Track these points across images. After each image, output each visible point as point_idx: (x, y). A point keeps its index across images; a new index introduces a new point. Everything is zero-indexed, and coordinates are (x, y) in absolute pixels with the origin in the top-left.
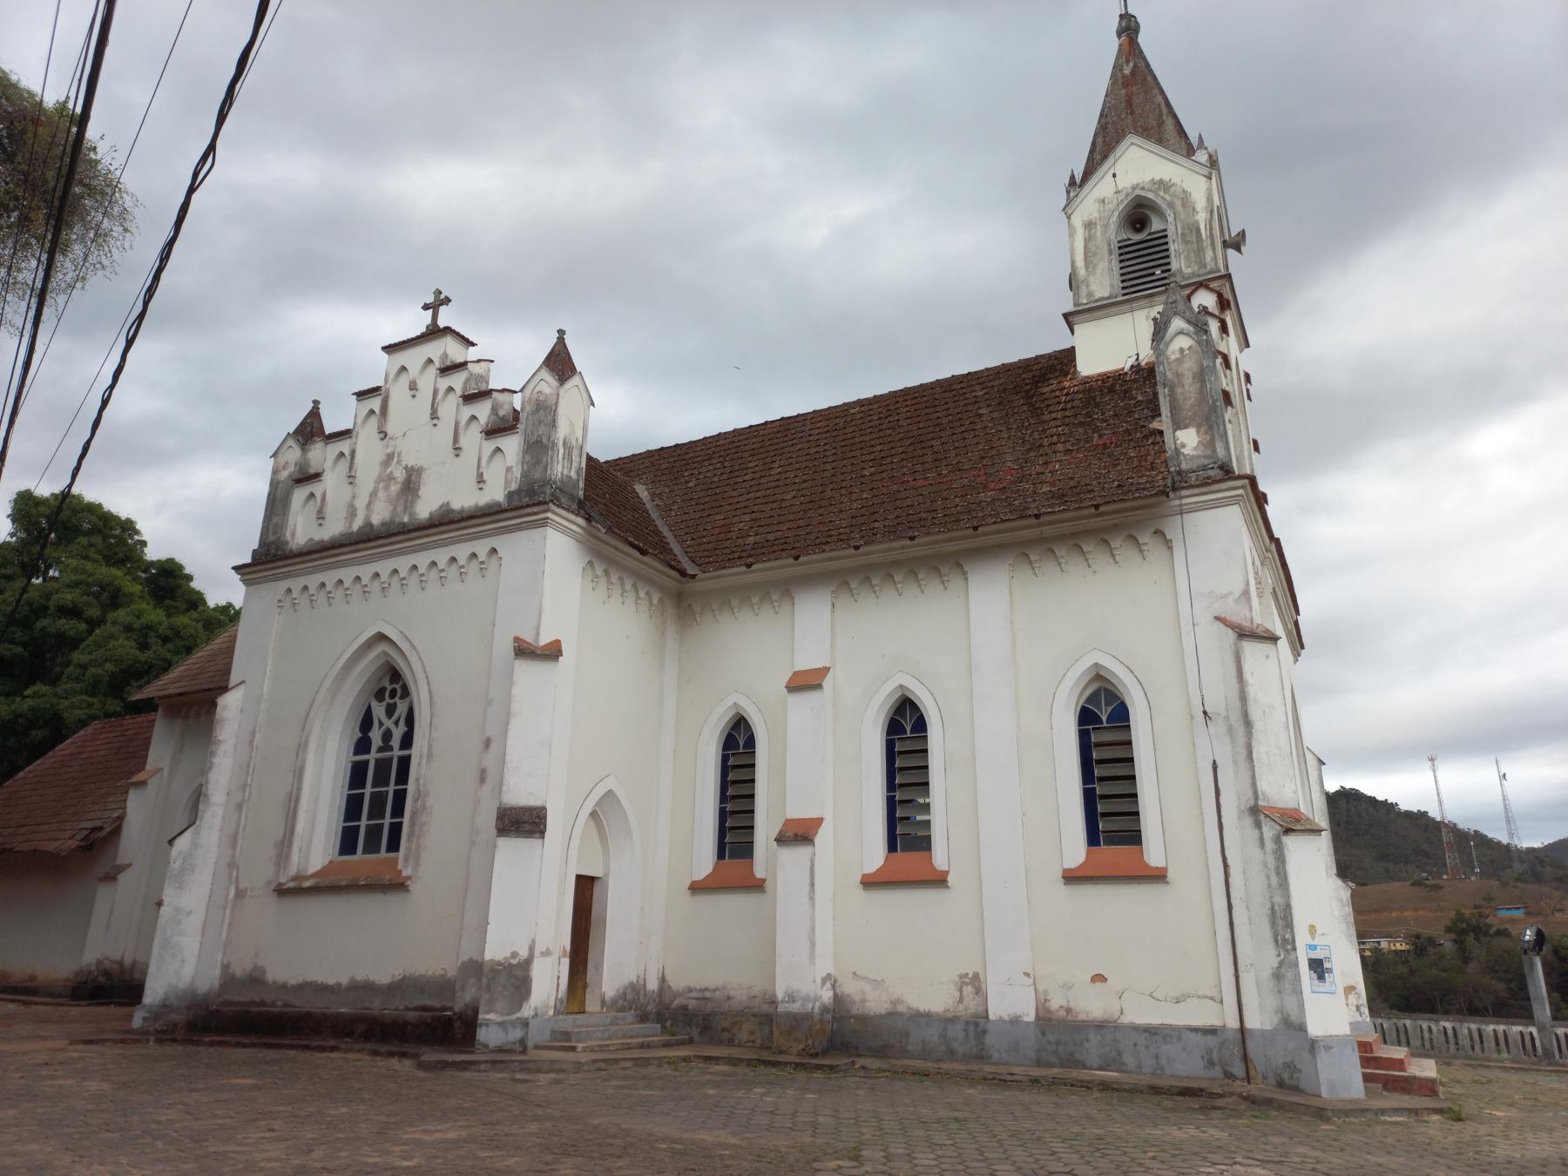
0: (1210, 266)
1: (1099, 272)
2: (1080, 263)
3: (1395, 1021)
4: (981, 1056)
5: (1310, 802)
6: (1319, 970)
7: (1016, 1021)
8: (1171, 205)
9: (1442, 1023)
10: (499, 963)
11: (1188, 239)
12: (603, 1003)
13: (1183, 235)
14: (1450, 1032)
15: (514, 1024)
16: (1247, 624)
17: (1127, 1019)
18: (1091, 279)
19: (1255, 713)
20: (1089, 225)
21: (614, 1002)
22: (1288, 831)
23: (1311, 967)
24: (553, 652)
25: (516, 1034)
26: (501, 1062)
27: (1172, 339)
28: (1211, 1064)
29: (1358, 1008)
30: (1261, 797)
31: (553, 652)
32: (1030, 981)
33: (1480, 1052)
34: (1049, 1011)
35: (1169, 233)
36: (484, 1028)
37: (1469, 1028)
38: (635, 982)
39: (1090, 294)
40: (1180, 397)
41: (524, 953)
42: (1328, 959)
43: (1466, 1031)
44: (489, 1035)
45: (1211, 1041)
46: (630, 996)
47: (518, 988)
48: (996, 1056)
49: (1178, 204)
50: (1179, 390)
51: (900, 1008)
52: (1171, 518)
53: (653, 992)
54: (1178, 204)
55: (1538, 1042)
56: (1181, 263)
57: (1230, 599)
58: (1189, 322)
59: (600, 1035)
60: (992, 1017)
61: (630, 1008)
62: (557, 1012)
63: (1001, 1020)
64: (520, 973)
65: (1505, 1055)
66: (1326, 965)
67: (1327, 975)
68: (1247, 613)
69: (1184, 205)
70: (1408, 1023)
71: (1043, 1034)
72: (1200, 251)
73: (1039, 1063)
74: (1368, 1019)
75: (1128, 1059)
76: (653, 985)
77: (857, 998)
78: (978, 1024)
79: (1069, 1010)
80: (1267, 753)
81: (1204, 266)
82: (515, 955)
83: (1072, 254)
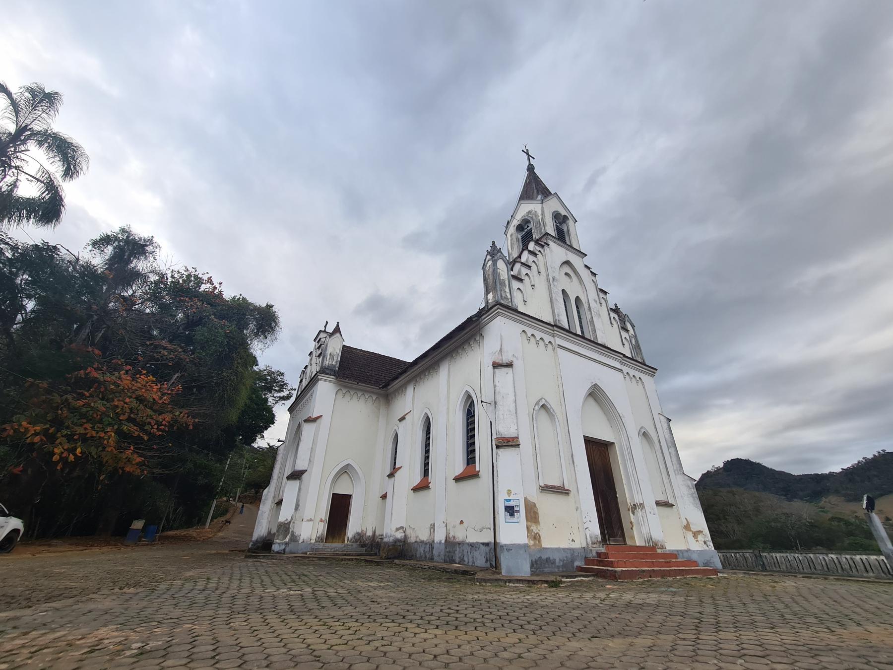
0: (544, 233)
1: (514, 248)
2: (510, 249)
3: (805, 555)
4: (432, 559)
5: (627, 438)
6: (510, 511)
7: (440, 543)
8: (532, 218)
9: (830, 555)
10: (282, 523)
11: (537, 226)
12: (348, 539)
13: (536, 226)
14: (836, 561)
15: (282, 543)
16: (501, 362)
17: (468, 541)
18: (513, 252)
19: (499, 398)
20: (511, 235)
21: (351, 539)
22: (498, 447)
23: (506, 510)
24: (315, 420)
25: (283, 547)
26: (267, 556)
27: (487, 264)
28: (487, 560)
29: (705, 542)
30: (498, 434)
31: (315, 420)
32: (444, 525)
33: (856, 573)
34: (449, 538)
35: (533, 228)
36: (274, 545)
37: (846, 558)
38: (360, 532)
39: (513, 258)
40: (489, 283)
41: (289, 520)
42: (518, 506)
43: (844, 560)
44: (275, 548)
45: (487, 549)
46: (357, 537)
47: (286, 531)
48: (435, 558)
49: (534, 216)
50: (488, 280)
51: (418, 540)
52: (486, 326)
53: (369, 536)
54: (534, 216)
55: (888, 565)
56: (536, 236)
57: (497, 353)
58: (490, 256)
59: (330, 550)
60: (435, 542)
61: (357, 542)
62: (316, 541)
63: (437, 543)
64: (287, 526)
65: (871, 574)
66: (516, 509)
67: (516, 514)
68: (501, 357)
69: (535, 216)
70: (812, 556)
71: (446, 548)
72: (541, 228)
73: (445, 562)
74: (713, 549)
75: (466, 559)
76: (369, 533)
77: (409, 536)
78: (431, 545)
79: (454, 537)
80: (503, 414)
81: (542, 233)
82: (287, 520)
83: (508, 247)
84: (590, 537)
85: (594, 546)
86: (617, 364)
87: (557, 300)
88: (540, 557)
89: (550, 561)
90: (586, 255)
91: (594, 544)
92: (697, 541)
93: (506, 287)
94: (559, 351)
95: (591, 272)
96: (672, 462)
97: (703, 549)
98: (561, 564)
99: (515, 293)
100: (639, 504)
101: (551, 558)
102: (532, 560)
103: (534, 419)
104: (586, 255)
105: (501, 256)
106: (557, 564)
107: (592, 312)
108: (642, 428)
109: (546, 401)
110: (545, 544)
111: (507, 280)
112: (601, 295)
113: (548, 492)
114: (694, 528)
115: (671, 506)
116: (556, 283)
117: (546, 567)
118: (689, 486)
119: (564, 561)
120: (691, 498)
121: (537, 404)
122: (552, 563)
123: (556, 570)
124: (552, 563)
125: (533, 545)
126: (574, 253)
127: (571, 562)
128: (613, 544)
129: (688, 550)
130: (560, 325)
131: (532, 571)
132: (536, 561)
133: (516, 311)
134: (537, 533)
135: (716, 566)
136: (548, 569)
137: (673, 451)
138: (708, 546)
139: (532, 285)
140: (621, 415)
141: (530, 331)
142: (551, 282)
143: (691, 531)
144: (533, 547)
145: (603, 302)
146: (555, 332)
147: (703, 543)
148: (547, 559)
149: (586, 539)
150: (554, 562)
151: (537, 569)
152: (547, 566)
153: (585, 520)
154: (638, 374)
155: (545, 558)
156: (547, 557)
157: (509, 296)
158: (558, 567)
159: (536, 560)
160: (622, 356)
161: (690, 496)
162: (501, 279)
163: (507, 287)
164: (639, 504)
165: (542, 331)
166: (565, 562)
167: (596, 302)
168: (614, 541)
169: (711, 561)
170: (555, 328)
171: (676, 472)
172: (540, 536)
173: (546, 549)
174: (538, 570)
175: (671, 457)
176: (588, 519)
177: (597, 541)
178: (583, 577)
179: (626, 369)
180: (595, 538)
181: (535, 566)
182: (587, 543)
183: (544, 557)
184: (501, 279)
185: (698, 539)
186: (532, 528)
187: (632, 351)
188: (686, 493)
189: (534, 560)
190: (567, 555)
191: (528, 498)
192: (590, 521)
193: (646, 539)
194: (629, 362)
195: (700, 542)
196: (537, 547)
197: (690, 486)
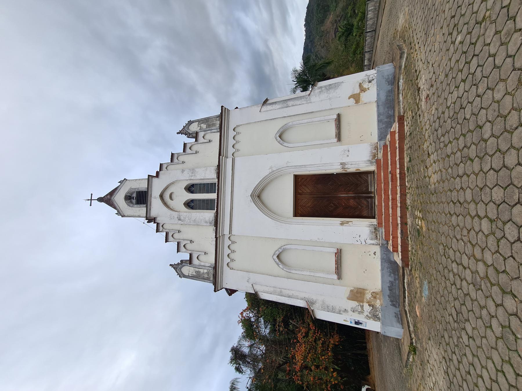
84: (372, 239)
85: (378, 237)
86: (229, 161)
87: (195, 220)
88: (389, 296)
90: (148, 175)
91: (377, 237)
92: (368, 89)
93: (200, 272)
94: (233, 233)
95: (160, 170)
96: (300, 105)
97: (376, 84)
98: (392, 275)
99: (202, 264)
100: (342, 166)
101: (389, 285)
102: (391, 305)
103: (290, 271)
104: (148, 175)
105: (179, 270)
106: (392, 279)
107: (193, 178)
109: (274, 254)
111: (195, 268)
112: (175, 160)
113: (341, 273)
114: (357, 90)
115: (339, 117)
116: (182, 218)
117: (396, 292)
118: (320, 92)
119: (390, 272)
120: (330, 91)
121: (278, 264)
123: (397, 282)
125: (380, 301)
126: (151, 187)
127: (391, 263)
128: (373, 188)
129: (377, 102)
130: (213, 222)
131: (398, 307)
132: (392, 301)
133: (215, 268)
134: (372, 294)
135: (392, 74)
136: (397, 290)
137: (290, 103)
138: (373, 80)
139: (191, 243)
140: (270, 171)
141: (227, 260)
142: (182, 223)
143: (359, 94)
144: (382, 301)
145: (181, 158)
146: (220, 235)
147: (370, 83)
148: (390, 290)
149: (373, 244)
150: (391, 283)
151: (397, 302)
153: (359, 243)
154: (232, 134)
155: (389, 291)
156: (387, 289)
157: (206, 271)
158: (395, 280)
159: (390, 301)
160: (221, 157)
161: (328, 92)
162: (195, 274)
163: (200, 270)
164: (342, 166)
165: (223, 241)
166: (391, 271)
167: (183, 171)
169: (387, 78)
170: (218, 236)
171: (309, 102)
172: (373, 292)
174: (397, 301)
175: (296, 105)
176: (358, 238)
177: (375, 232)
178: (405, 279)
179: (231, 150)
180: (373, 234)
181: (394, 303)
182: (376, 245)
183: (388, 292)
184: (195, 274)
185: (367, 87)
186: (368, 298)
187: (212, 131)
188: (326, 95)
189: (390, 303)
190: (386, 266)
191: (347, 295)
193: (370, 164)
194: (224, 147)
195: (369, 86)
196: (382, 297)
197: (319, 90)
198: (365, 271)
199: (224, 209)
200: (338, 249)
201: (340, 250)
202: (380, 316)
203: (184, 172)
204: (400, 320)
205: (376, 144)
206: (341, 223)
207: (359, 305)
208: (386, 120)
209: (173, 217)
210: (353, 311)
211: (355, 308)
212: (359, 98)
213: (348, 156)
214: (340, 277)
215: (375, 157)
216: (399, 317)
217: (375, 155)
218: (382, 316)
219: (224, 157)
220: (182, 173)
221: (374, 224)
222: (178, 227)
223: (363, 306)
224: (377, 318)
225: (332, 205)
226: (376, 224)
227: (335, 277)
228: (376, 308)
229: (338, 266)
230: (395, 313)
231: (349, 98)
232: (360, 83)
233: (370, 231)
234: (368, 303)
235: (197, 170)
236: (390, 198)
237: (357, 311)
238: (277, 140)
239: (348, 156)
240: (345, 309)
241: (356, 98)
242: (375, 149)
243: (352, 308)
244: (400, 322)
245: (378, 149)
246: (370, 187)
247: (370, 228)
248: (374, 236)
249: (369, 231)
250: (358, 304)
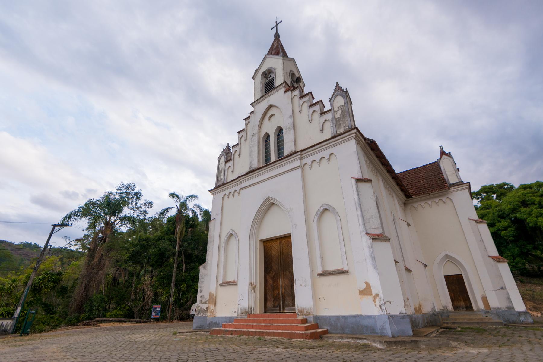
85: (242, 315)
88: (212, 322)
89: (217, 323)
91: (243, 313)
108: (322, 206)
110: (218, 315)
116: (254, 138)
122: (218, 325)
124: (218, 325)
128: (288, 312)
132: (210, 324)
143: (371, 294)
144: (209, 317)
152: (215, 326)
156: (216, 321)
159: (210, 323)
168: (289, 310)
173: (219, 317)
177: (245, 312)
180: (244, 310)
183: (214, 321)
186: (211, 307)
189: (209, 323)
191: (211, 292)
192: (243, 300)
195: (377, 306)
198: (225, 304)
199: (259, 175)
200: (236, 282)
201: (236, 284)
202: (200, 315)
203: (290, 119)
204: (198, 328)
205: (312, 313)
206: (253, 283)
207: (206, 300)
208: (339, 325)
209: (254, 129)
210: (201, 297)
211: (204, 298)
212: (366, 295)
213: (301, 285)
214: (221, 285)
215: (300, 313)
216: (201, 328)
217: (302, 312)
218: (200, 316)
219: (300, 156)
220: (289, 117)
221: (252, 311)
222: (249, 137)
223: (206, 303)
224: (198, 313)
225: (274, 274)
226: (252, 313)
227: (221, 282)
228: (205, 313)
229: (232, 283)
230: (203, 326)
231: (366, 283)
232: (378, 295)
233: (246, 308)
234: (209, 307)
235: (292, 131)
236: (253, 324)
237: (202, 299)
238: (320, 207)
239: (301, 285)
240: (202, 291)
241: (366, 291)
242: (307, 313)
243: (204, 295)
244: (197, 329)
245: (307, 315)
246: (288, 309)
247: (248, 308)
248: (243, 311)
249: (246, 307)
250: (207, 299)
